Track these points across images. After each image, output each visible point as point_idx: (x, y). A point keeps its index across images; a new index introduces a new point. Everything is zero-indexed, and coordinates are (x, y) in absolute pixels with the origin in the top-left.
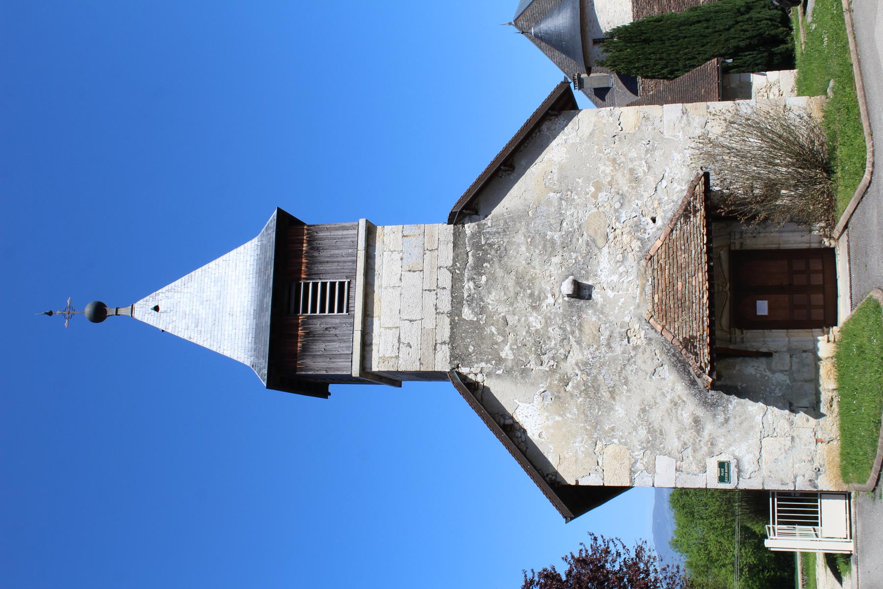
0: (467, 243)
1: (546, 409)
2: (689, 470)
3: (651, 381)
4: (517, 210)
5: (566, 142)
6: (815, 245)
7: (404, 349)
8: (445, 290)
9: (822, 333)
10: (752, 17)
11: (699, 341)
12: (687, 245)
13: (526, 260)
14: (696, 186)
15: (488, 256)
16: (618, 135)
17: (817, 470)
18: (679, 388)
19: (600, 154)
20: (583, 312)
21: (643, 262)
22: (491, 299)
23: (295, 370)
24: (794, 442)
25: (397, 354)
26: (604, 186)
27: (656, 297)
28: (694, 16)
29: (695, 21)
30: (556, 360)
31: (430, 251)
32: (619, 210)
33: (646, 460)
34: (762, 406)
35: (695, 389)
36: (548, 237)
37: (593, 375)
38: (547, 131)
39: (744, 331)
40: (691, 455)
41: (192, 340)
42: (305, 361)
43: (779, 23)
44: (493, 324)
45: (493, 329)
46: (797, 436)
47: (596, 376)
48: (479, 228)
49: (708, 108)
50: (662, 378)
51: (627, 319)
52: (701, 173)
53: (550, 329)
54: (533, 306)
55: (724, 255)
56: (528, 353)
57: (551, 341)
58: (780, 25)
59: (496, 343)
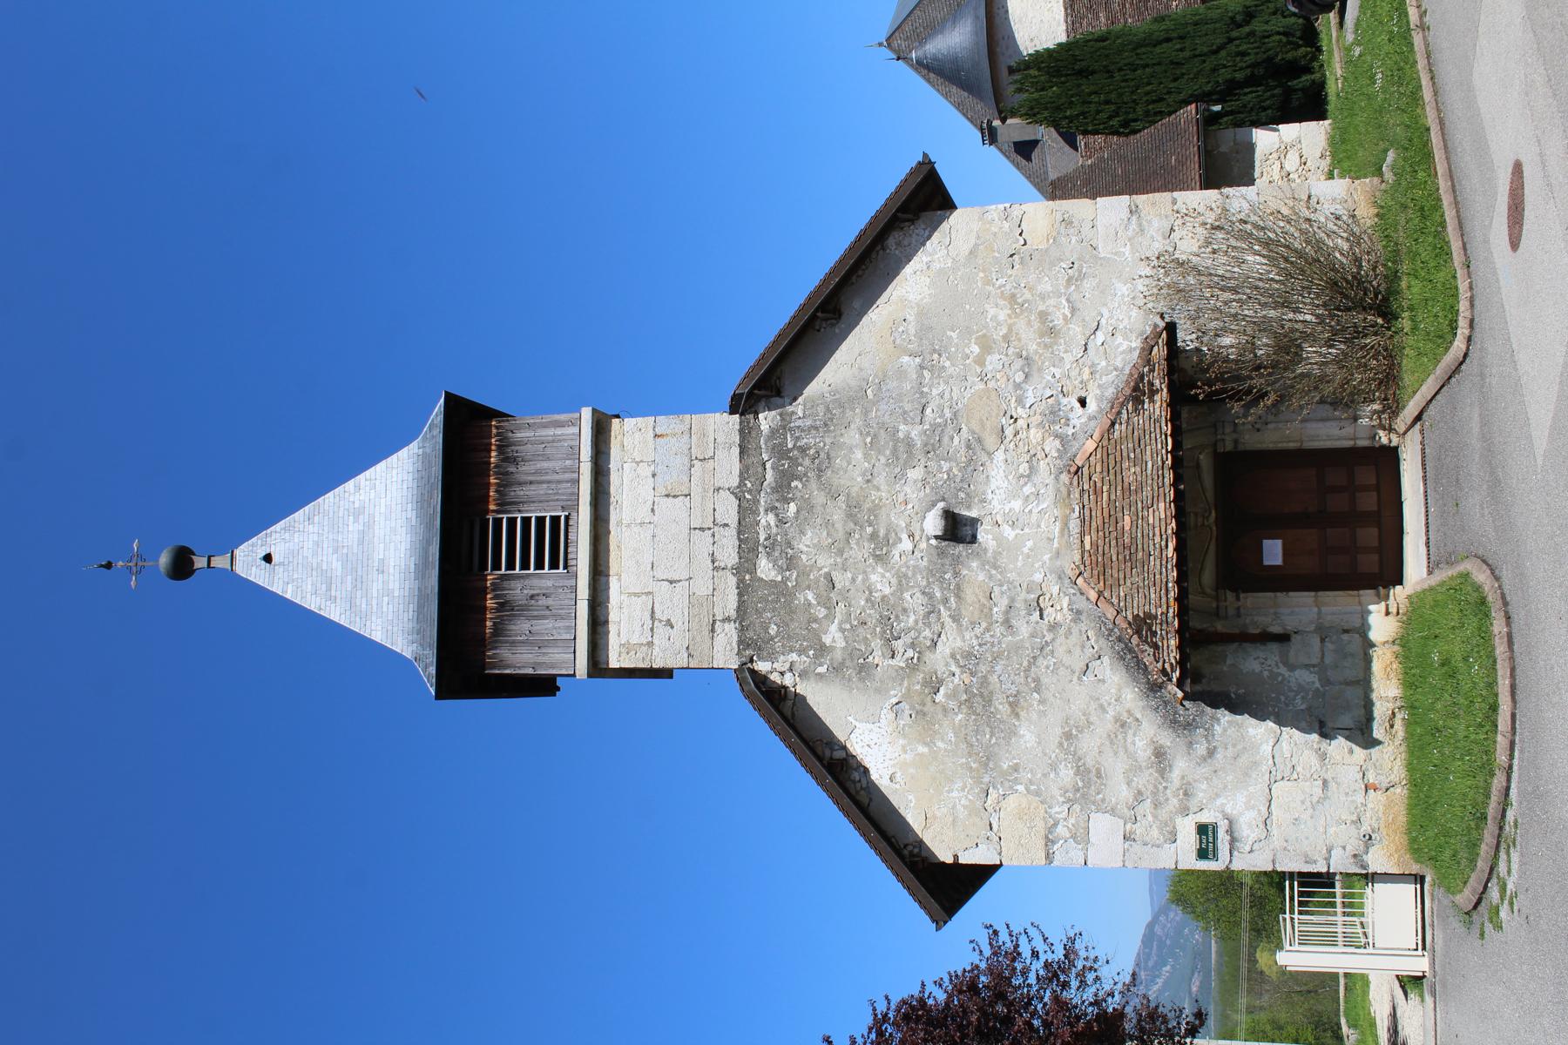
0: (763, 446)
1: (902, 733)
2: (1147, 839)
3: (1080, 685)
4: (847, 389)
5: (928, 268)
7: (660, 630)
8: (727, 528)
9: (1376, 599)
10: (1256, 31)
11: (1161, 624)
12: (1138, 451)
13: (864, 475)
14: (1153, 346)
15: (799, 468)
16: (1019, 253)
17: (1367, 837)
18: (1129, 696)
19: (987, 287)
20: (962, 563)
21: (1065, 478)
22: (806, 544)
23: (484, 666)
24: (1327, 790)
25: (650, 639)
26: (995, 343)
27: (1087, 539)
28: (1161, 31)
29: (1161, 38)
30: (918, 650)
31: (701, 460)
32: (1023, 385)
33: (1072, 820)
34: (1272, 728)
35: (1156, 698)
36: (901, 435)
37: (980, 675)
38: (896, 249)
39: (1242, 595)
40: (1151, 813)
41: (322, 613)
42: (498, 651)
43: (1300, 38)
44: (809, 588)
45: (810, 596)
46: (1333, 779)
47: (985, 677)
48: (783, 419)
49: (1174, 202)
51: (1038, 577)
52: (1162, 324)
53: (907, 595)
54: (877, 556)
55: (1205, 460)
56: (869, 636)
57: (908, 616)
58: (1301, 43)
59: (815, 621)
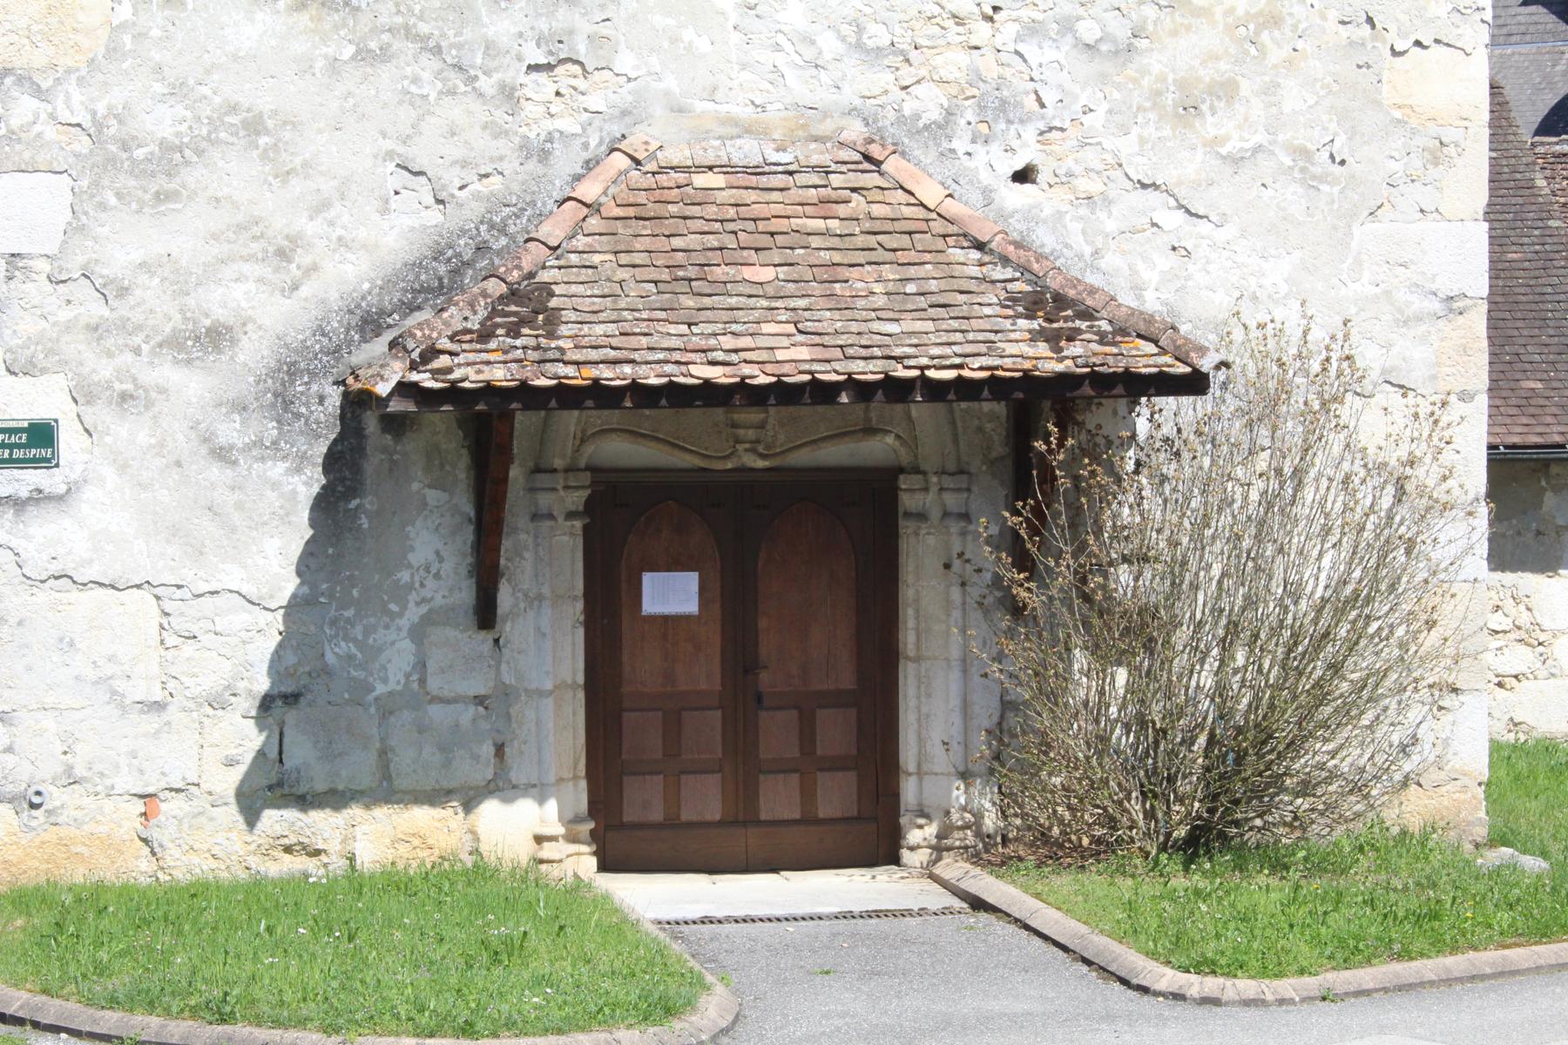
3: (376, 156)
6: (909, 791)
9: (570, 815)
12: (922, 302)
14: (1156, 342)
16: (1374, 38)
17: (36, 800)
18: (349, 268)
21: (855, 131)
24: (142, 712)
27: (715, 180)
32: (1069, 39)
35: (348, 331)
39: (578, 524)
46: (168, 723)
49: (1465, 397)
50: (387, 201)
51: (625, 62)
52: (1206, 364)
55: (878, 449)
